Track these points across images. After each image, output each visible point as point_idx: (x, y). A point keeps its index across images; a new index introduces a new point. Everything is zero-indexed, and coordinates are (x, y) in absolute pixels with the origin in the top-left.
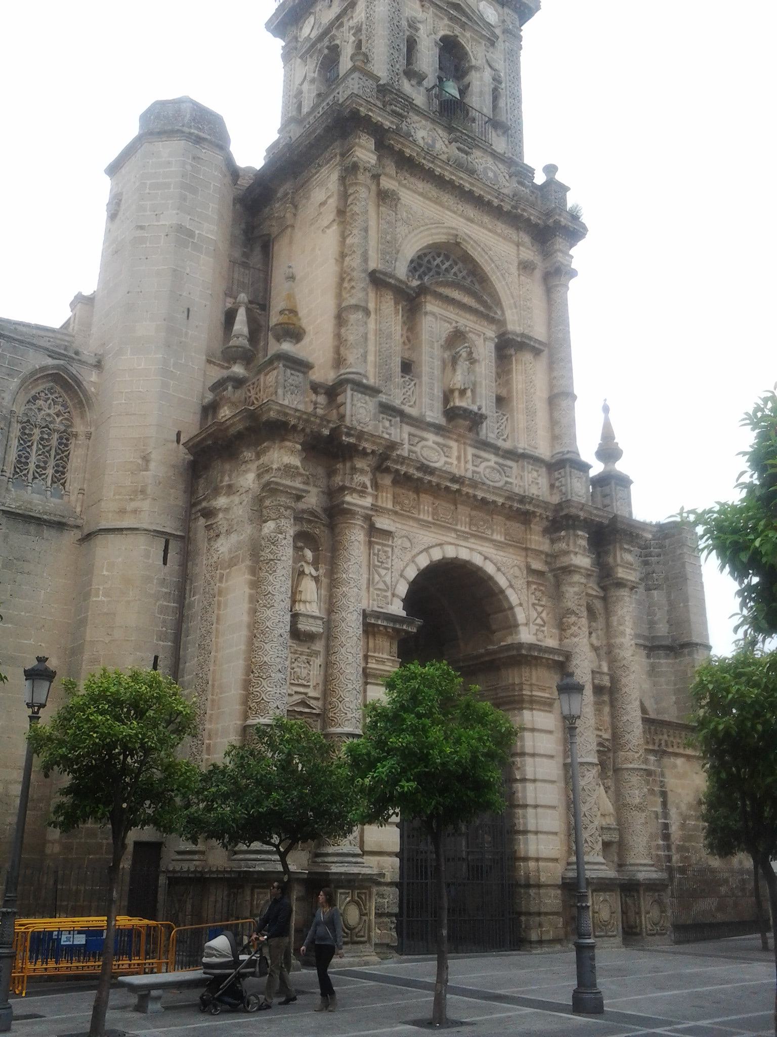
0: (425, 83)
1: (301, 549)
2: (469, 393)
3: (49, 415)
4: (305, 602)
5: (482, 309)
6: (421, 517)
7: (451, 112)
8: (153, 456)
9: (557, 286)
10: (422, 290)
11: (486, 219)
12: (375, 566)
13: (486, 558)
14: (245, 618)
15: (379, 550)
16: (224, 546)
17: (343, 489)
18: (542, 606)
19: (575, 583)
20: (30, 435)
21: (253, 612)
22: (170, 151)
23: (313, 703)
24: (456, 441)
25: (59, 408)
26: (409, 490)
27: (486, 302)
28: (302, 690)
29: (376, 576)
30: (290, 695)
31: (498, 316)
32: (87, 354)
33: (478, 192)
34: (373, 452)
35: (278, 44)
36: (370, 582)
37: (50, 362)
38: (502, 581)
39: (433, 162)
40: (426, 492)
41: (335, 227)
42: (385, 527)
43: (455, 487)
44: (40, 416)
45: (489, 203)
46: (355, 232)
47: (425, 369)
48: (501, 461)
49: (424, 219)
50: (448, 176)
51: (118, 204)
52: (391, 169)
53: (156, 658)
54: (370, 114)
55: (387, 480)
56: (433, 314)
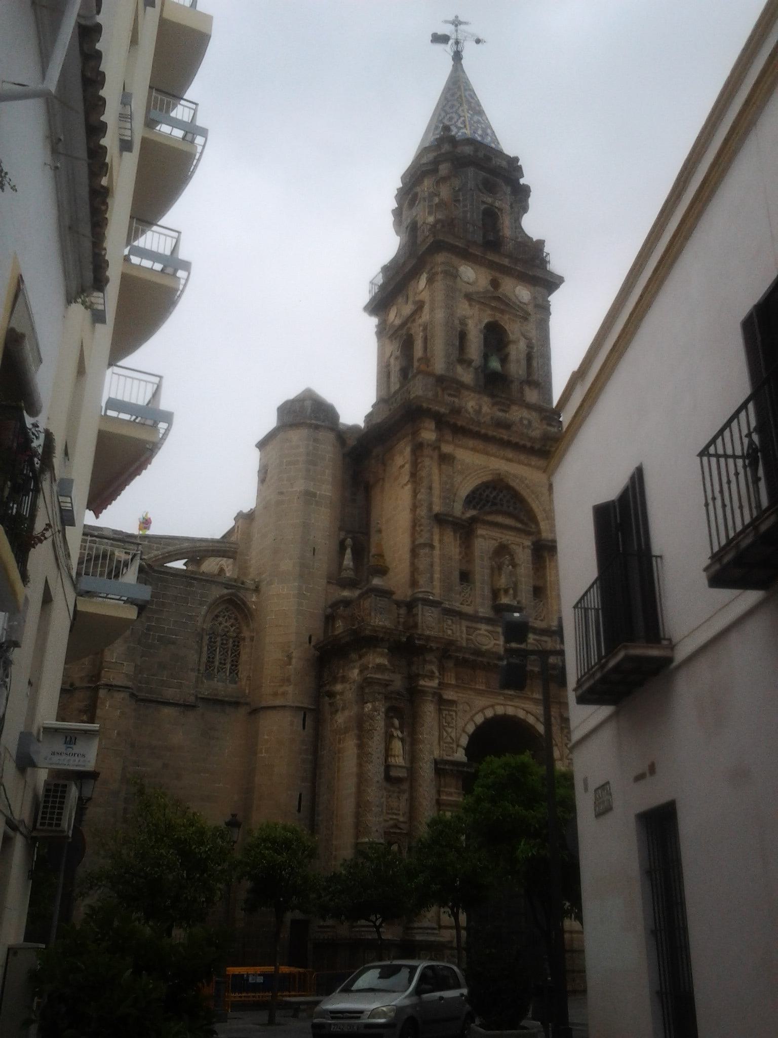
0: (473, 364)
1: (392, 717)
2: (511, 592)
3: (226, 627)
4: (394, 756)
5: (519, 525)
6: (477, 687)
7: (495, 383)
8: (294, 655)
10: (473, 520)
11: (522, 457)
12: (444, 726)
13: (527, 712)
14: (355, 770)
16: (341, 719)
17: (418, 675)
20: (215, 642)
21: (360, 765)
22: (297, 437)
23: (402, 826)
25: (232, 621)
28: (395, 817)
29: (445, 733)
30: (386, 821)
31: (533, 528)
32: (249, 583)
33: (514, 439)
34: (438, 648)
35: (371, 323)
36: (440, 737)
41: (409, 486)
42: (450, 698)
44: (221, 628)
45: (524, 446)
46: (422, 490)
47: (478, 577)
48: (537, 637)
49: (475, 465)
50: (490, 433)
51: (266, 472)
52: (449, 437)
53: (300, 795)
55: (450, 664)
56: (482, 536)
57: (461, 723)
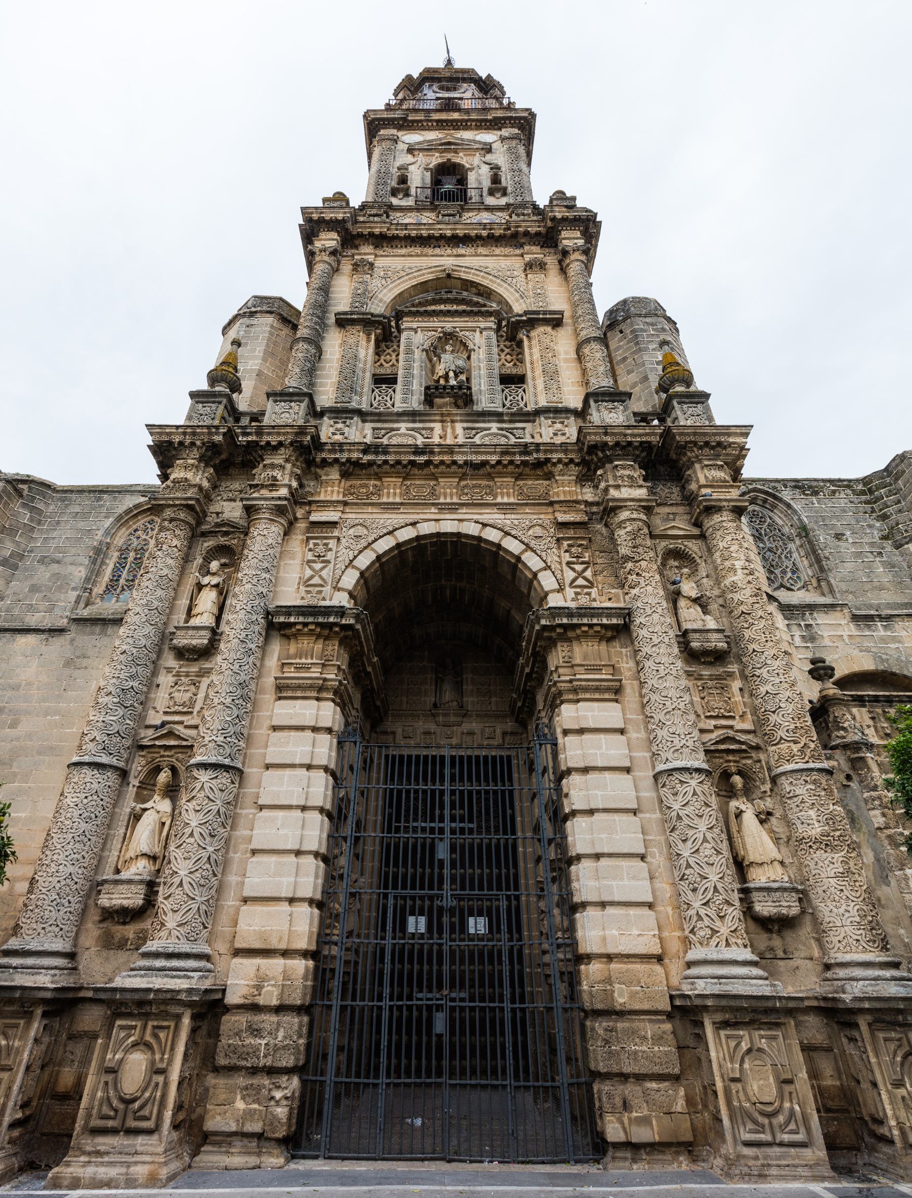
9: (568, 265)
13: (485, 525)
15: (315, 544)
18: (582, 563)
19: (624, 521)
24: (442, 421)
26: (370, 479)
27: (478, 303)
37: (142, 499)
38: (512, 546)
40: (388, 474)
43: (422, 459)
57: (346, 555)
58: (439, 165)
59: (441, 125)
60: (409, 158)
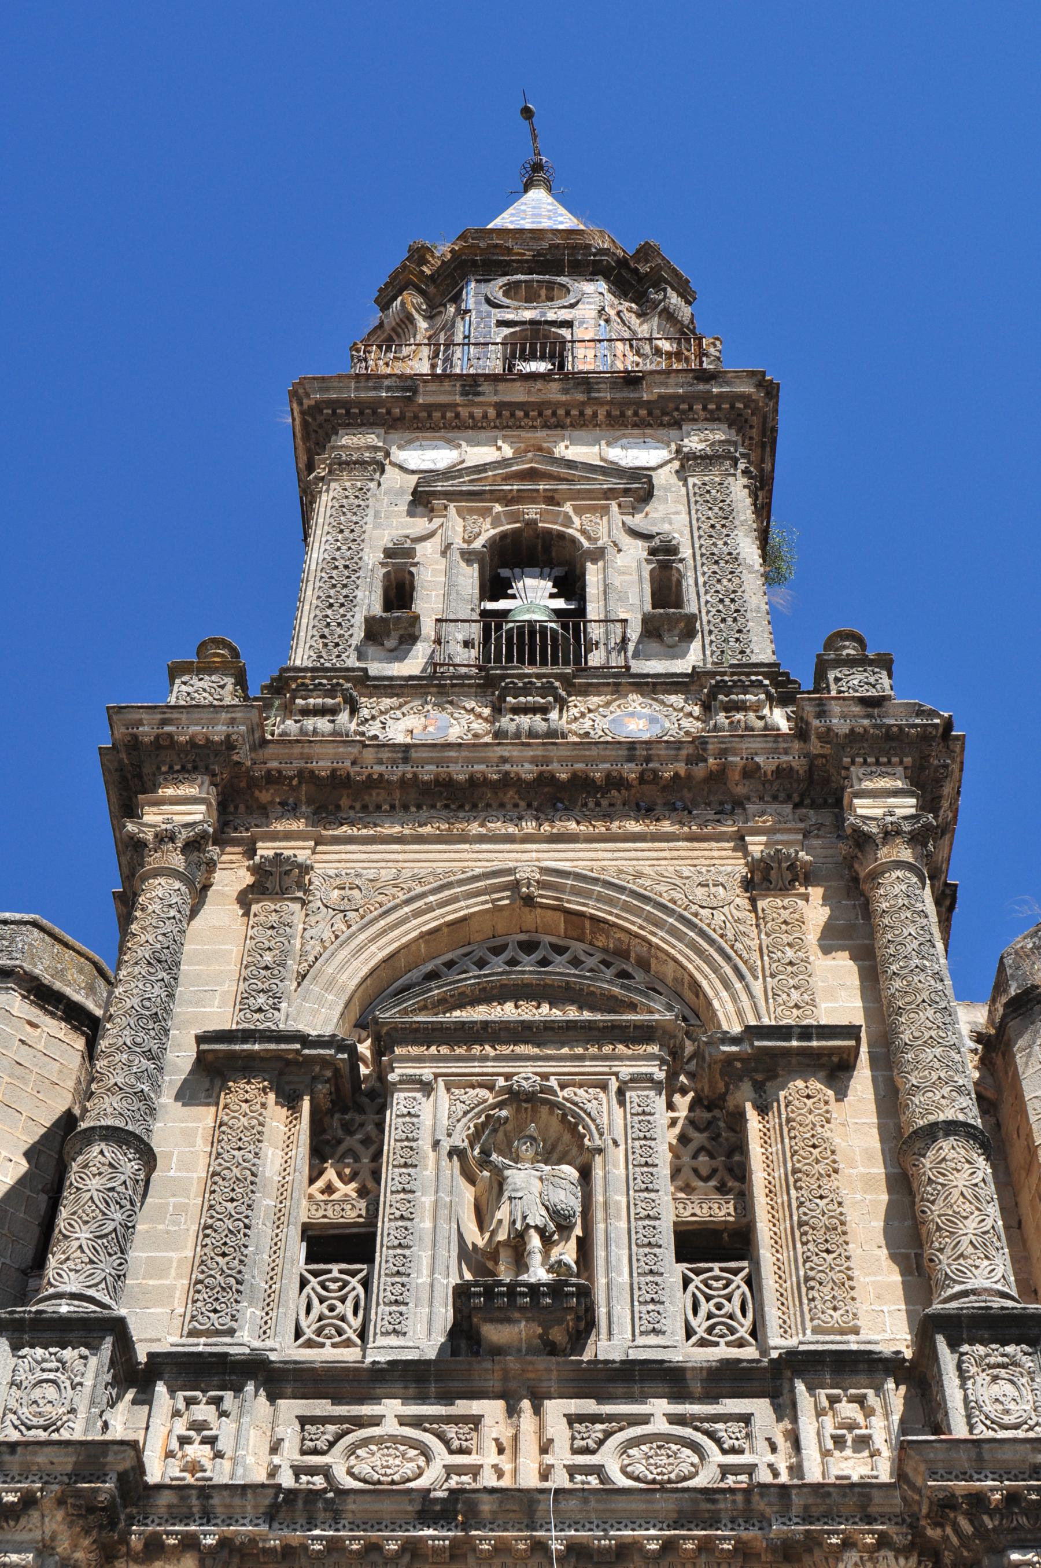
9: (875, 876)
39: (406, 760)
54: (168, 729)
58: (503, 536)
59: (508, 419)
60: (420, 525)
